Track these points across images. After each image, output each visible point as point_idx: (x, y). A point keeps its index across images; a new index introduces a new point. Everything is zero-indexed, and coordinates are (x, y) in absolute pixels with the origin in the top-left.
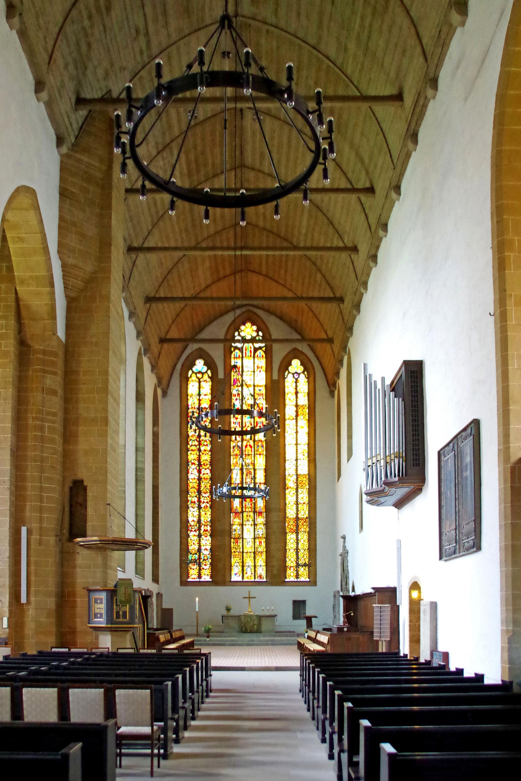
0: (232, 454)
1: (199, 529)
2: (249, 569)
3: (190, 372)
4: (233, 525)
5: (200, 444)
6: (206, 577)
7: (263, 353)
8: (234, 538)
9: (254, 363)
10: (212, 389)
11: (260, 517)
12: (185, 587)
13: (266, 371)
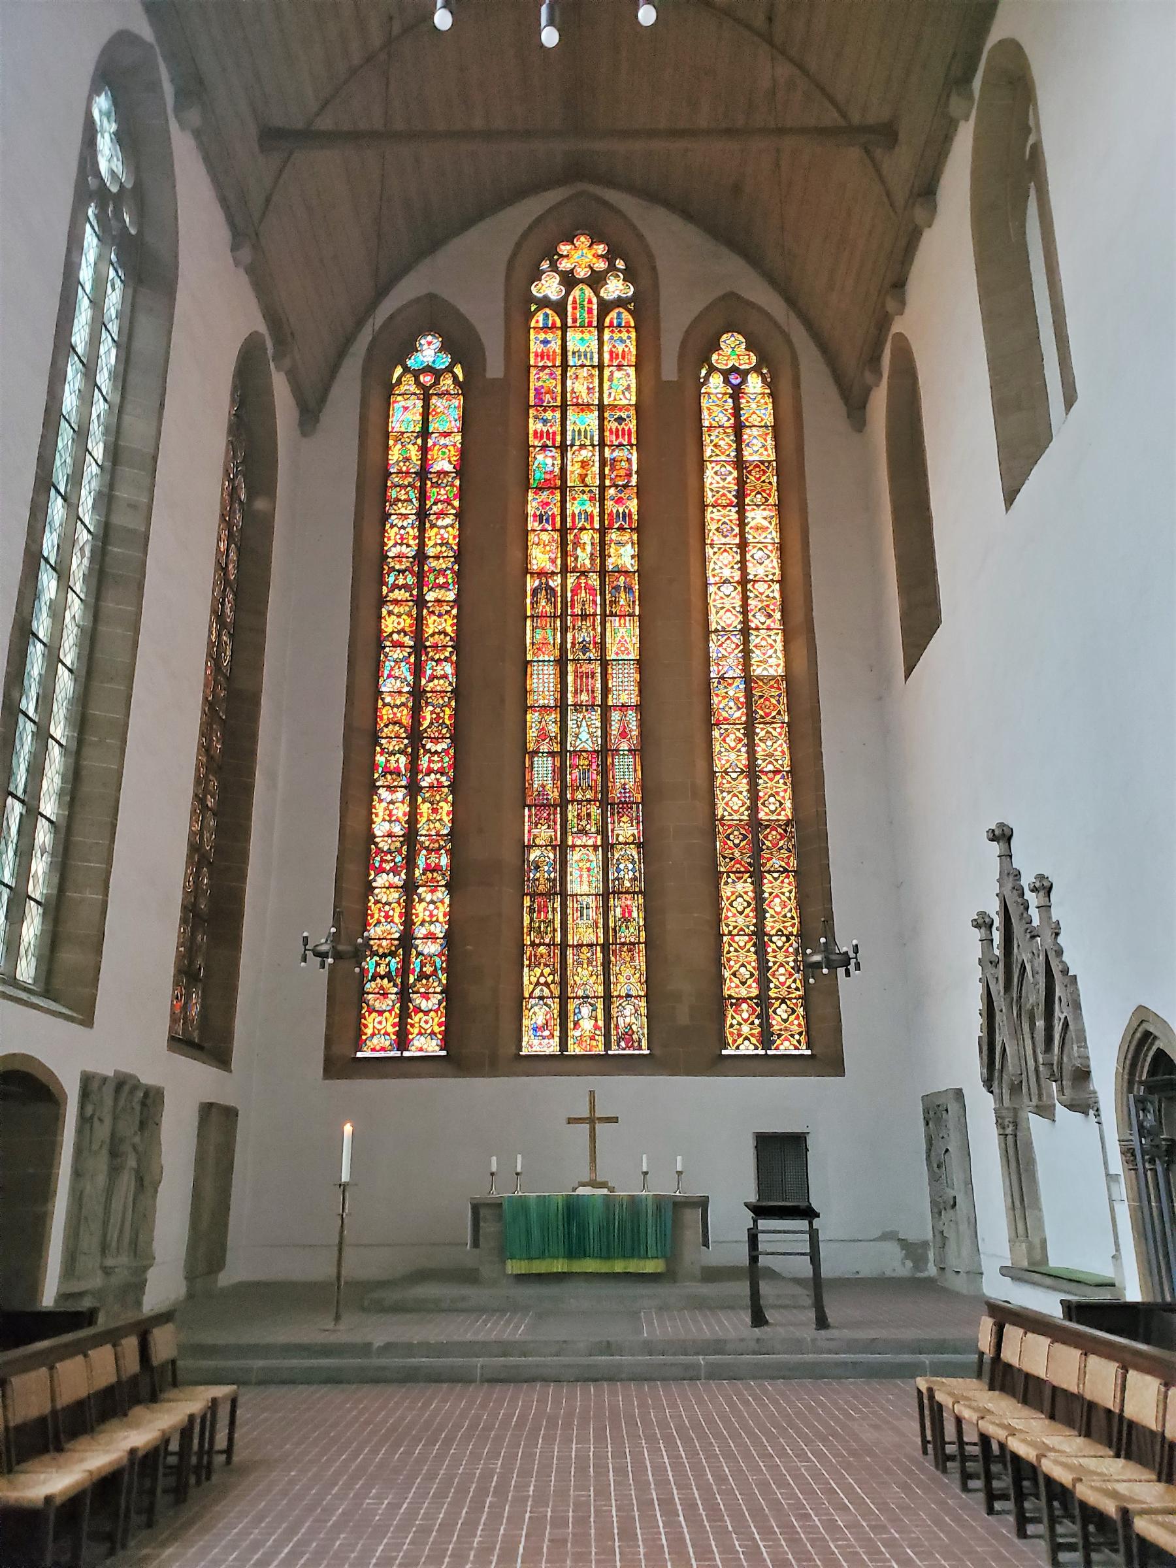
0: (529, 614)
1: (410, 862)
3: (399, 370)
4: (530, 847)
5: (420, 584)
6: (426, 1045)
7: (627, 317)
8: (533, 896)
9: (601, 343)
10: (465, 419)
11: (625, 819)
12: (342, 1085)
13: (638, 367)
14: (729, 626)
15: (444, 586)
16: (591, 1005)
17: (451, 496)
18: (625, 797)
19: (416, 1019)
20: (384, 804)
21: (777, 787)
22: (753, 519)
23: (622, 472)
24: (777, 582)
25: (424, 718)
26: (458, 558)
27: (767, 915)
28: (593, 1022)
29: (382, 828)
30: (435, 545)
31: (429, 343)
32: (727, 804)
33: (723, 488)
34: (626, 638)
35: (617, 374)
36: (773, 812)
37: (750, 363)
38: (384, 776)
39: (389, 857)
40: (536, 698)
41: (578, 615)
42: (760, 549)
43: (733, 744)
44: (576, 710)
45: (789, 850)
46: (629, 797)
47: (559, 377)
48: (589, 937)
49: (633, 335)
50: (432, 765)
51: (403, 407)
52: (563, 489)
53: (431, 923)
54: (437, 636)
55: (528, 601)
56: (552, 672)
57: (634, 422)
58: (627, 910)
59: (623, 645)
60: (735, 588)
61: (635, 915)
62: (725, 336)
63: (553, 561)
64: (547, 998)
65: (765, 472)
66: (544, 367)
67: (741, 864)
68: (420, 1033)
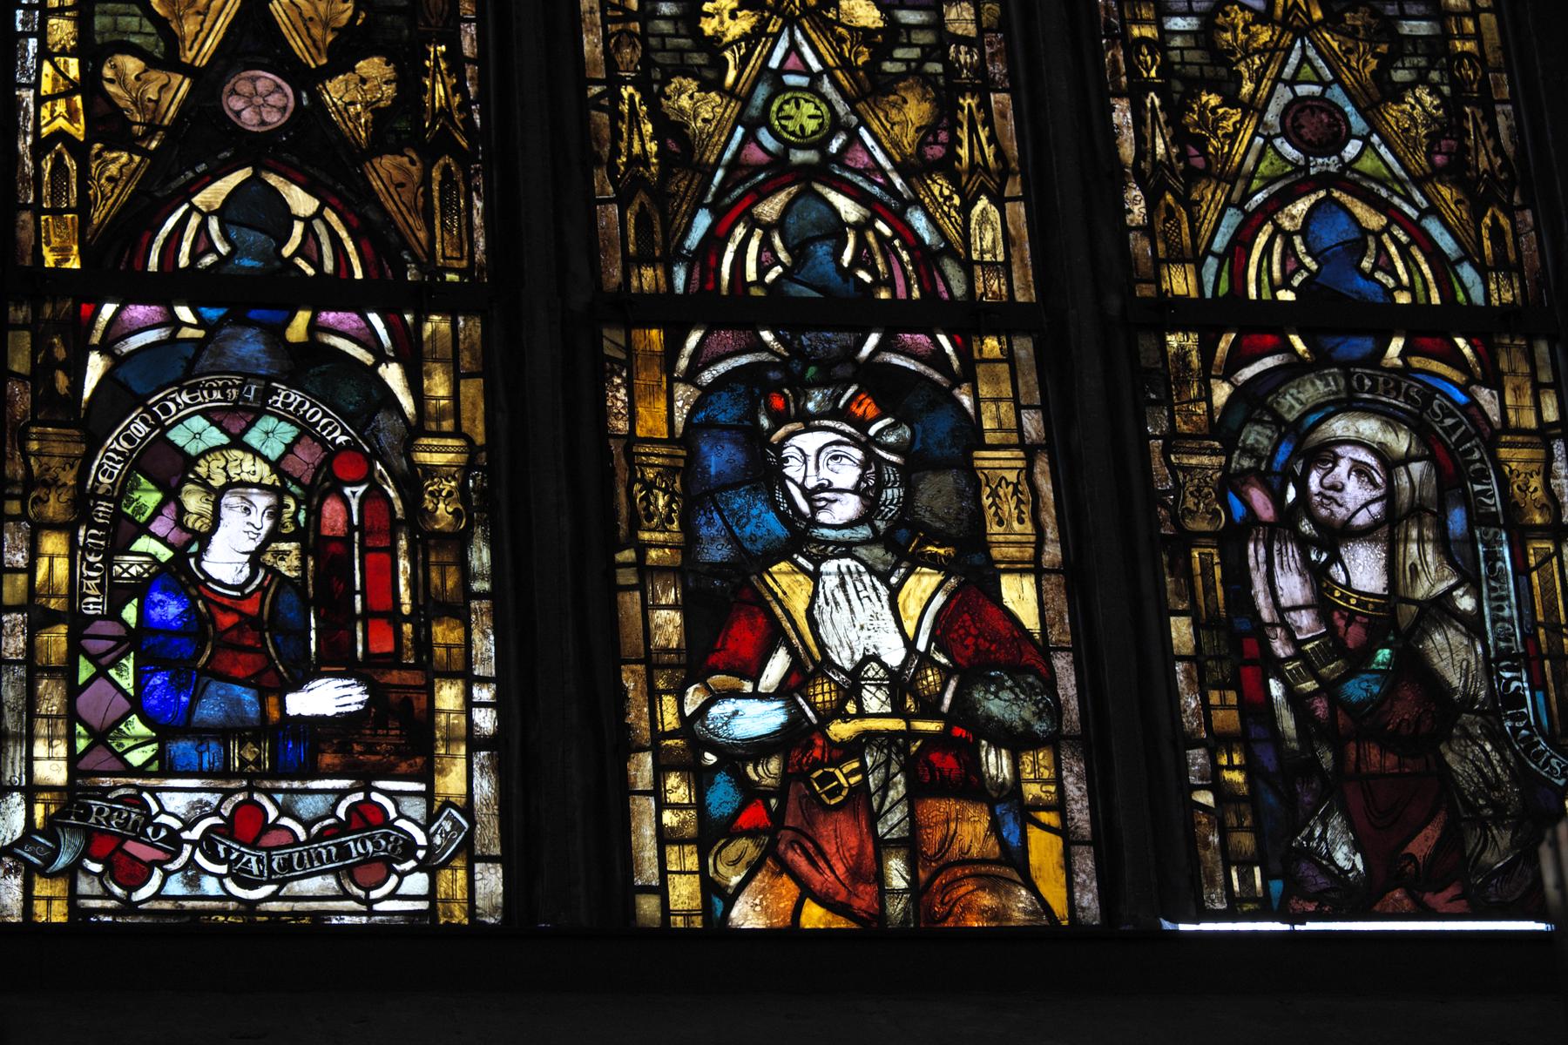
28: (921, 587)
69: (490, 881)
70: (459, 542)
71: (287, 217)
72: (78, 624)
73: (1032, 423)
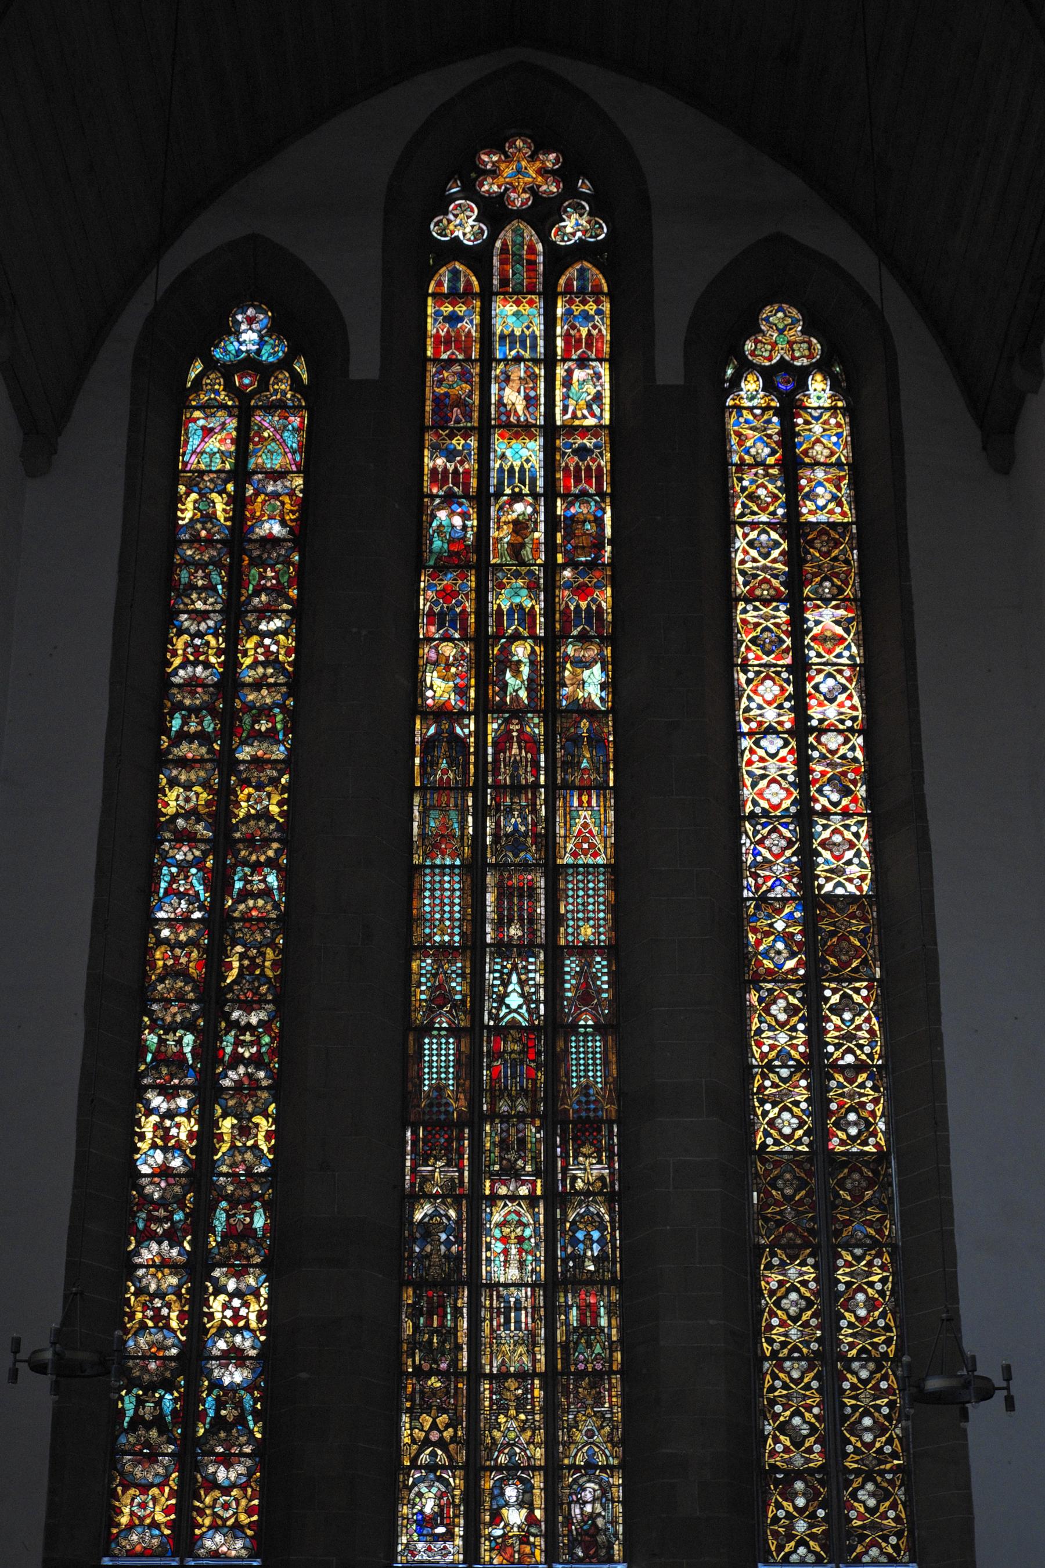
2: (511, 1492)
3: (197, 368)
7: (597, 277)
8: (419, 1286)
14: (776, 807)
15: (270, 735)
16: (522, 1480)
17: (284, 579)
18: (588, 1110)
19: (208, 1500)
20: (154, 1119)
21: (861, 1095)
22: (817, 623)
23: (585, 541)
24: (860, 732)
25: (230, 968)
26: (293, 687)
27: (843, 1323)
28: (524, 1512)
29: (151, 1161)
30: (255, 664)
31: (250, 321)
32: (771, 1123)
33: (764, 569)
34: (592, 826)
35: (579, 375)
36: (853, 1139)
37: (810, 357)
38: (156, 1068)
39: (162, 1213)
40: (427, 931)
41: (505, 786)
42: (830, 675)
43: (782, 1017)
44: (500, 955)
45: (882, 1207)
46: (595, 1110)
47: (476, 379)
48: (519, 1359)
49: (606, 307)
50: (240, 1050)
51: (203, 428)
52: (483, 570)
53: (236, 1330)
54: (252, 823)
55: (417, 761)
56: (457, 886)
57: (608, 456)
58: (589, 1311)
59: (585, 840)
60: (786, 743)
61: (603, 1322)
62: (768, 308)
63: (461, 691)
64: (443, 1467)
65: (837, 544)
66: (451, 362)
67: (795, 1231)
68: (214, 1527)
69: (461, 1557)
70: (459, 1506)
71: (437, 1455)
72: (408, 1519)
73: (542, 1485)
